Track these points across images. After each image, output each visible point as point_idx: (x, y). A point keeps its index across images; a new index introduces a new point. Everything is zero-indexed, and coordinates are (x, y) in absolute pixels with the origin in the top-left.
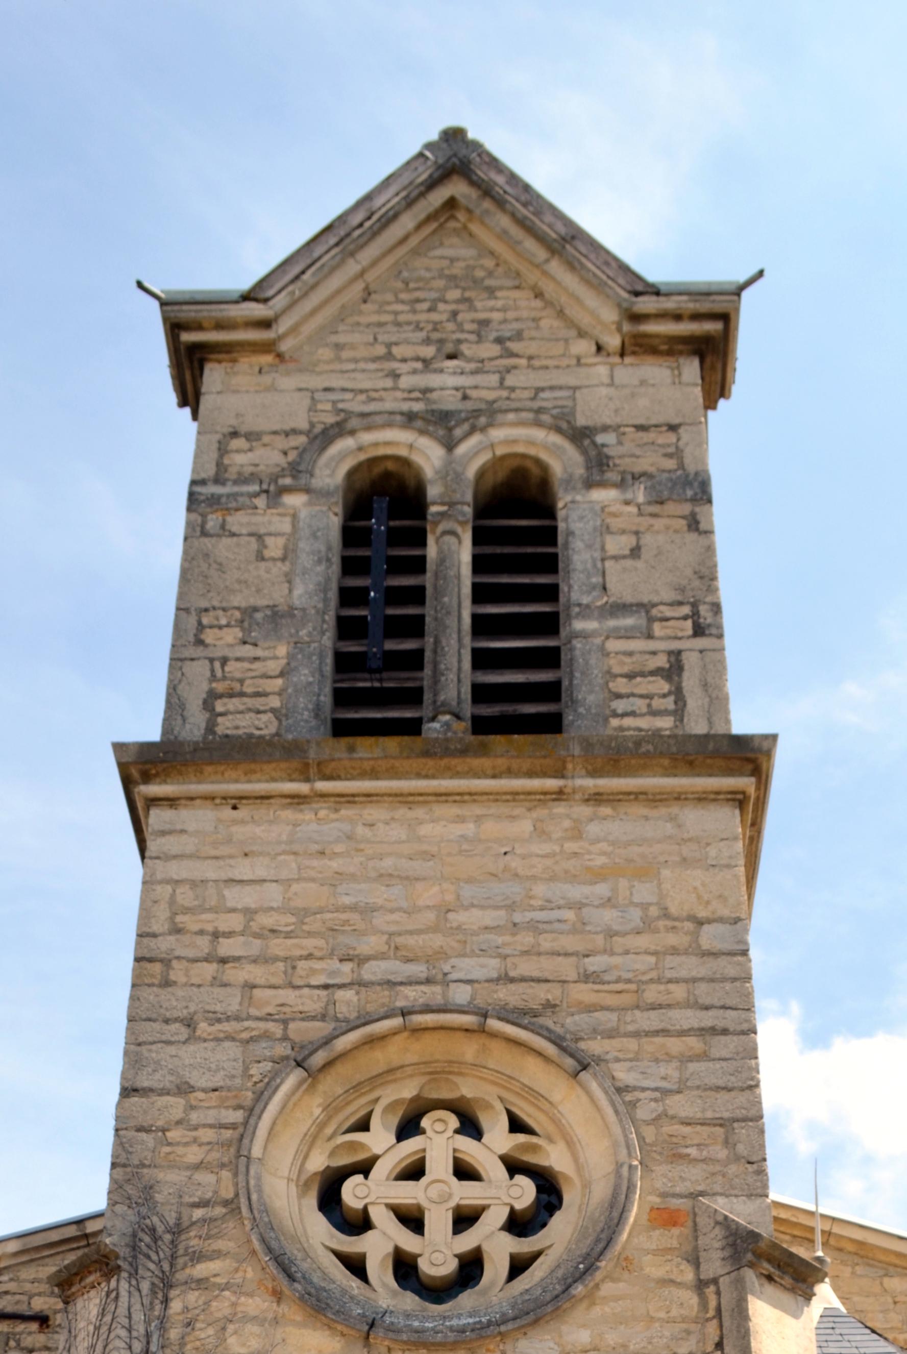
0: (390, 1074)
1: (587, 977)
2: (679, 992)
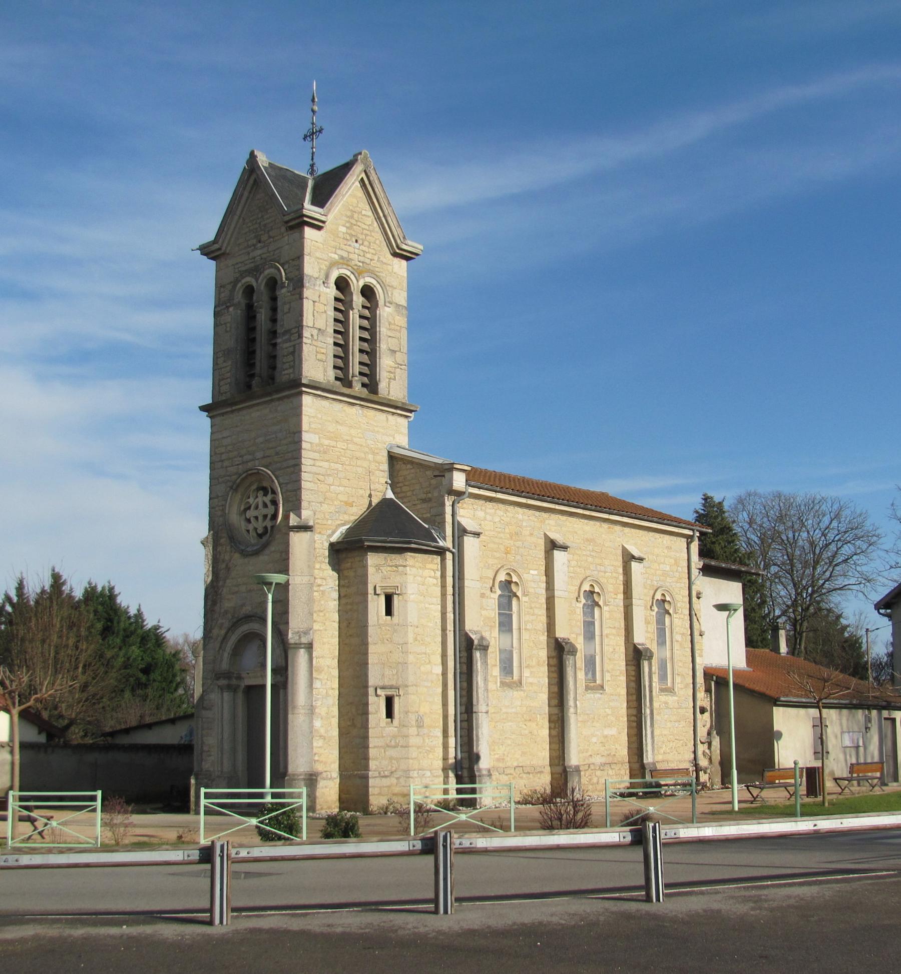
0: (250, 486)
1: (277, 454)
2: (290, 455)
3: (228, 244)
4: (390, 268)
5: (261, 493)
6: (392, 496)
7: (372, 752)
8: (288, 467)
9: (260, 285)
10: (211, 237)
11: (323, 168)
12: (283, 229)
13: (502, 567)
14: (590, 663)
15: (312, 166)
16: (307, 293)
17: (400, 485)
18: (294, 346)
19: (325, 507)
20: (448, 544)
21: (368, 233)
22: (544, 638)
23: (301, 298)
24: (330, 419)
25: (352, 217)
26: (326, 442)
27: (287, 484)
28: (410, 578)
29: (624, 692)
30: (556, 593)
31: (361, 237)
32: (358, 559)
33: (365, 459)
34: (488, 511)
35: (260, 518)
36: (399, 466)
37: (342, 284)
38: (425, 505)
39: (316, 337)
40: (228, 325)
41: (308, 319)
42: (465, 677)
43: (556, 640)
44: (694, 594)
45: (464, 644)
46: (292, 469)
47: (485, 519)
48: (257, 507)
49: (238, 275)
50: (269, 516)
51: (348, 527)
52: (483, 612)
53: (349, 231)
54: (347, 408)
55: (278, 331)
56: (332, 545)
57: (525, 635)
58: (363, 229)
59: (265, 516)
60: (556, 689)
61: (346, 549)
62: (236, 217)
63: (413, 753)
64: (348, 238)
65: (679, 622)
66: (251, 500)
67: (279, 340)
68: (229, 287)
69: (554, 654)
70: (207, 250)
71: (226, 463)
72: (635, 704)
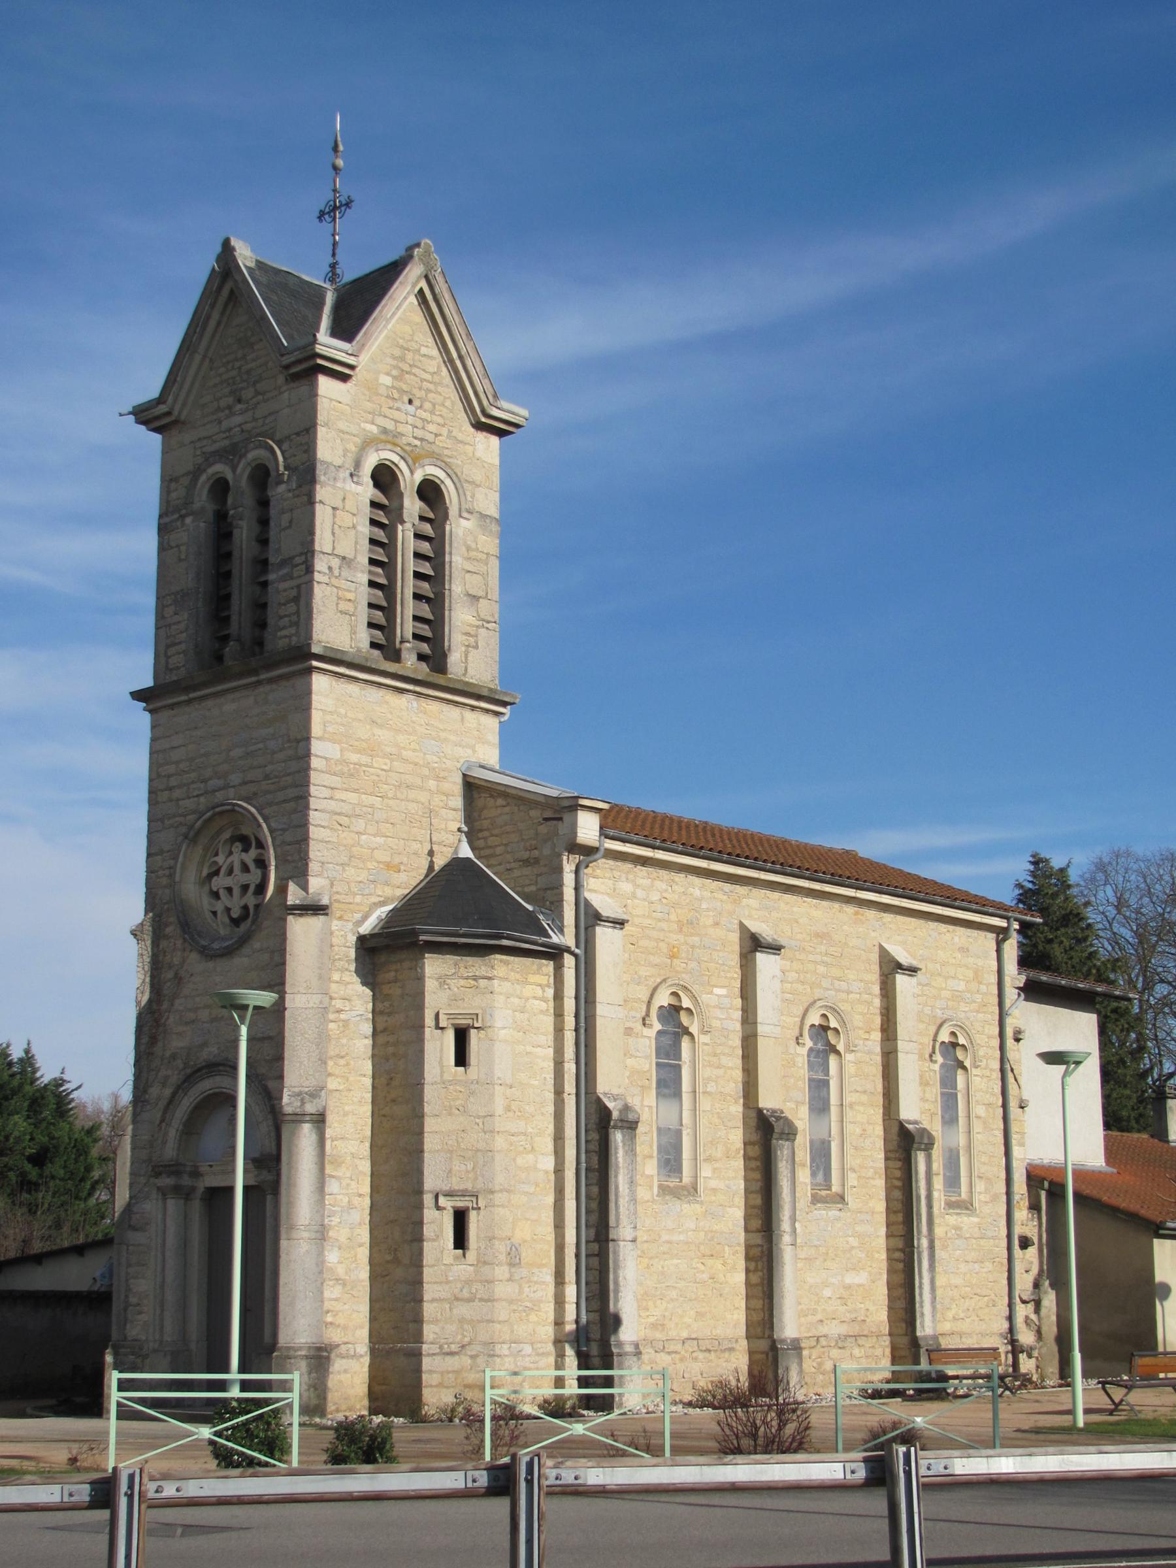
0: (219, 833)
1: (267, 777)
3: (184, 404)
4: (469, 449)
5: (238, 846)
6: (470, 855)
7: (429, 1310)
8: (285, 801)
9: (239, 477)
10: (154, 392)
11: (350, 272)
12: (281, 379)
13: (664, 980)
14: (821, 1154)
15: (333, 266)
16: (321, 493)
17: (486, 834)
18: (299, 586)
19: (350, 872)
20: (568, 939)
21: (431, 387)
22: (737, 1109)
23: (311, 502)
24: (361, 716)
25: (402, 359)
26: (354, 757)
27: (284, 830)
28: (499, 1001)
29: (881, 1206)
30: (761, 1029)
31: (419, 394)
32: (406, 964)
33: (421, 788)
34: (640, 881)
35: (236, 891)
36: (481, 800)
37: (384, 478)
38: (527, 871)
39: (336, 572)
40: (183, 548)
41: (323, 540)
42: (595, 1176)
43: (760, 1111)
44: (1009, 1032)
45: (594, 1118)
46: (292, 804)
47: (634, 896)
48: (230, 872)
49: (200, 460)
50: (252, 888)
51: (390, 907)
52: (629, 1062)
53: (398, 384)
55: (272, 560)
56: (362, 940)
57: (705, 1104)
58: (422, 380)
59: (245, 888)
60: (758, 1200)
61: (387, 948)
62: (198, 358)
63: (502, 1312)
64: (396, 395)
65: (981, 1082)
66: (220, 859)
67: (272, 577)
68: (186, 481)
69: (755, 1137)
70: (145, 415)
71: (177, 793)
72: (900, 1229)
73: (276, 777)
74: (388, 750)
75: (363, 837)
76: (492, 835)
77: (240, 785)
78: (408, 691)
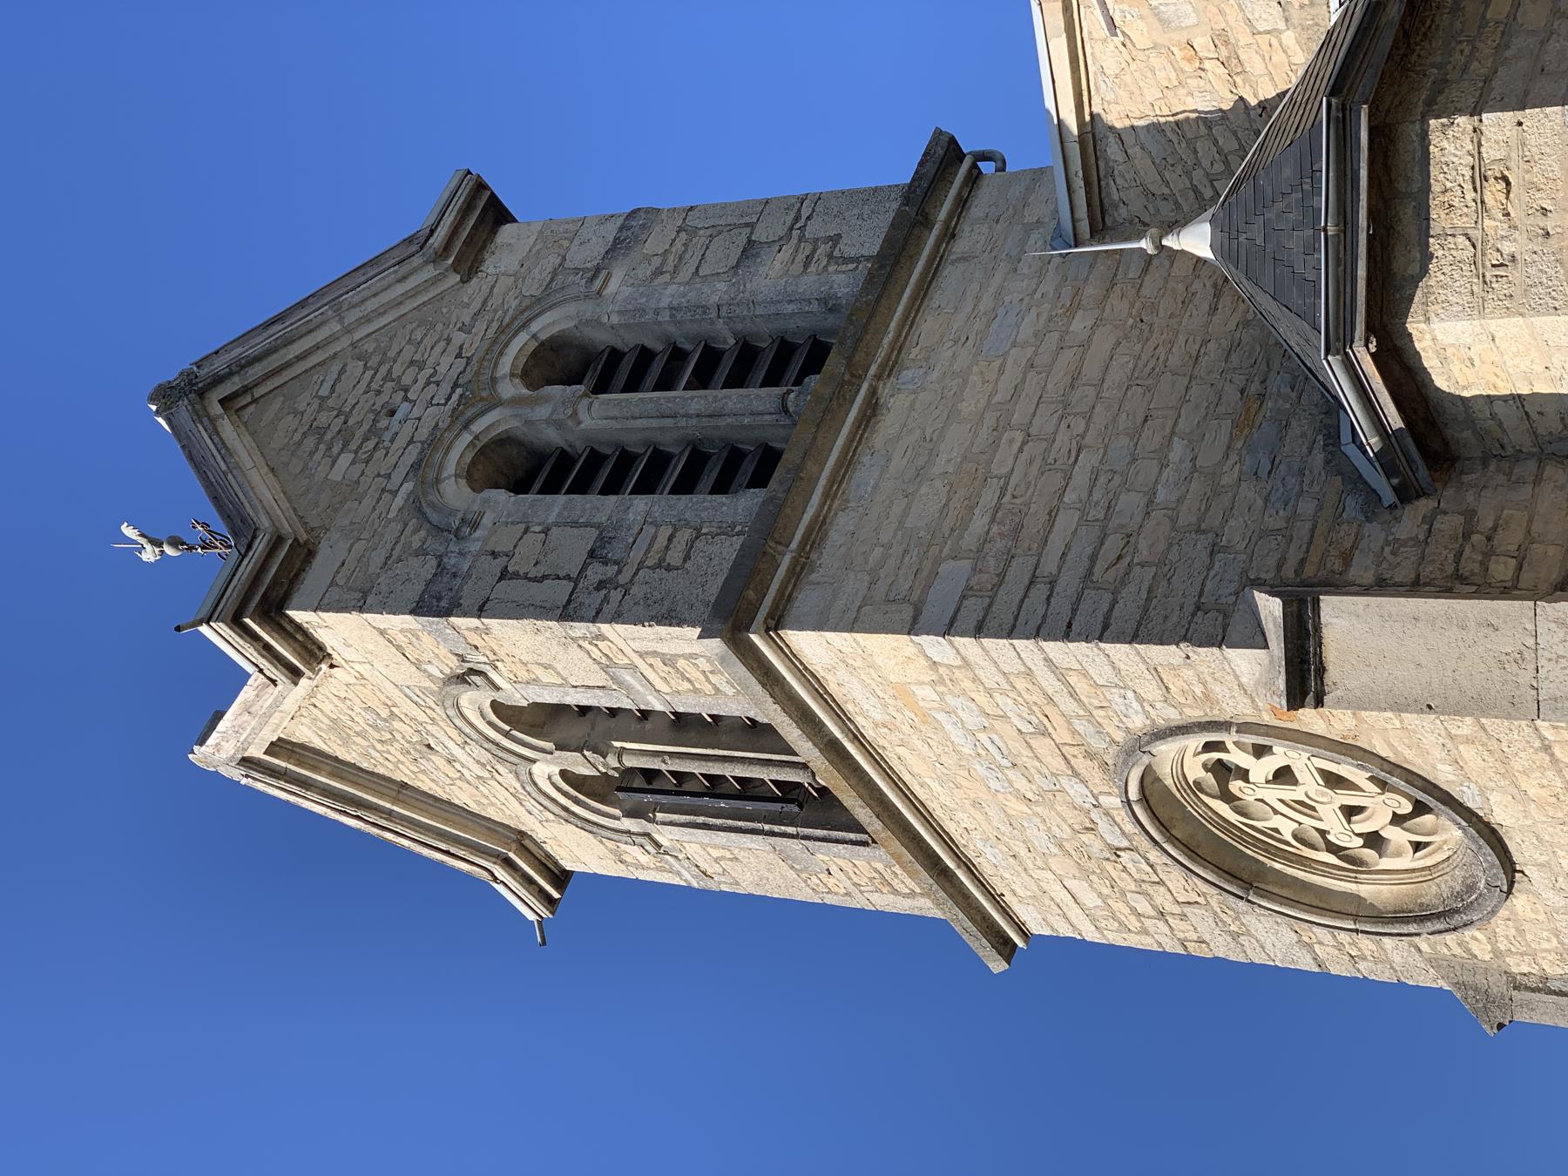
8: (1073, 694)
18: (641, 655)
19: (1235, 534)
21: (383, 371)
24: (897, 510)
25: (321, 432)
26: (979, 523)
27: (1140, 699)
31: (384, 398)
54: (887, 425)
64: (370, 444)
73: (1032, 712)
74: (984, 434)
75: (1161, 496)
76: (1197, 164)
77: (1084, 782)
78: (873, 392)
